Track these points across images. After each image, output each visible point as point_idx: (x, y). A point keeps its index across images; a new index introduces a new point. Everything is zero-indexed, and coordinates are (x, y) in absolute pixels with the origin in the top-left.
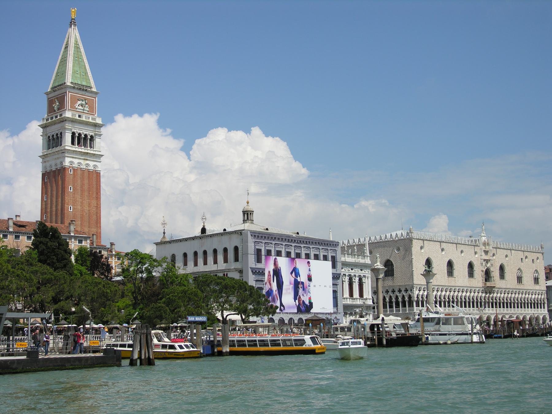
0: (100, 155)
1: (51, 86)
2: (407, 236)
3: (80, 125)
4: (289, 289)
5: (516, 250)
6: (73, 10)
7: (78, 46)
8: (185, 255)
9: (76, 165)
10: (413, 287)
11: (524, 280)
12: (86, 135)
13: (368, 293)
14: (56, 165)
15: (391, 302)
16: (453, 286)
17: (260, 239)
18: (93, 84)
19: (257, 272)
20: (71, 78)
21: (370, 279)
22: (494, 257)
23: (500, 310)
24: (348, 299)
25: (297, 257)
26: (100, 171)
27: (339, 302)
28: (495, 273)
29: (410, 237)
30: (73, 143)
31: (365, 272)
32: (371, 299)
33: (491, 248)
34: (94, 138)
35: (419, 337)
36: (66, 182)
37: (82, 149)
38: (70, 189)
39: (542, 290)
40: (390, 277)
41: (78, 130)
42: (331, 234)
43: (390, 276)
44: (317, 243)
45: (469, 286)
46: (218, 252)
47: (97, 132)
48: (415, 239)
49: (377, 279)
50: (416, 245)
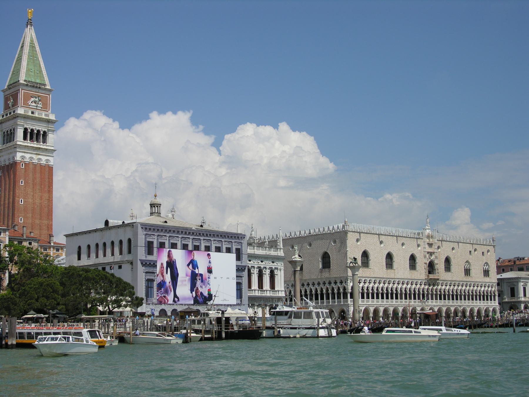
0: (52, 150)
1: (7, 84)
2: (342, 229)
3: (33, 121)
4: (186, 281)
5: (464, 243)
6: (30, 11)
7: (33, 45)
8: (89, 247)
9: (27, 160)
10: (347, 279)
11: (472, 272)
12: (39, 131)
13: (280, 285)
14: (9, 159)
17: (152, 232)
18: (47, 81)
19: (148, 264)
20: (25, 76)
21: (282, 272)
22: (439, 250)
24: (256, 291)
26: (52, 165)
27: (243, 294)
28: (440, 266)
29: (346, 229)
30: (25, 138)
31: (277, 264)
32: (283, 291)
34: (47, 134)
35: (260, 331)
36: (17, 176)
37: (34, 144)
38: (21, 183)
40: (327, 269)
41: (30, 126)
42: (239, 226)
44: (219, 236)
45: (410, 278)
47: (50, 127)
48: (350, 232)
50: (351, 238)
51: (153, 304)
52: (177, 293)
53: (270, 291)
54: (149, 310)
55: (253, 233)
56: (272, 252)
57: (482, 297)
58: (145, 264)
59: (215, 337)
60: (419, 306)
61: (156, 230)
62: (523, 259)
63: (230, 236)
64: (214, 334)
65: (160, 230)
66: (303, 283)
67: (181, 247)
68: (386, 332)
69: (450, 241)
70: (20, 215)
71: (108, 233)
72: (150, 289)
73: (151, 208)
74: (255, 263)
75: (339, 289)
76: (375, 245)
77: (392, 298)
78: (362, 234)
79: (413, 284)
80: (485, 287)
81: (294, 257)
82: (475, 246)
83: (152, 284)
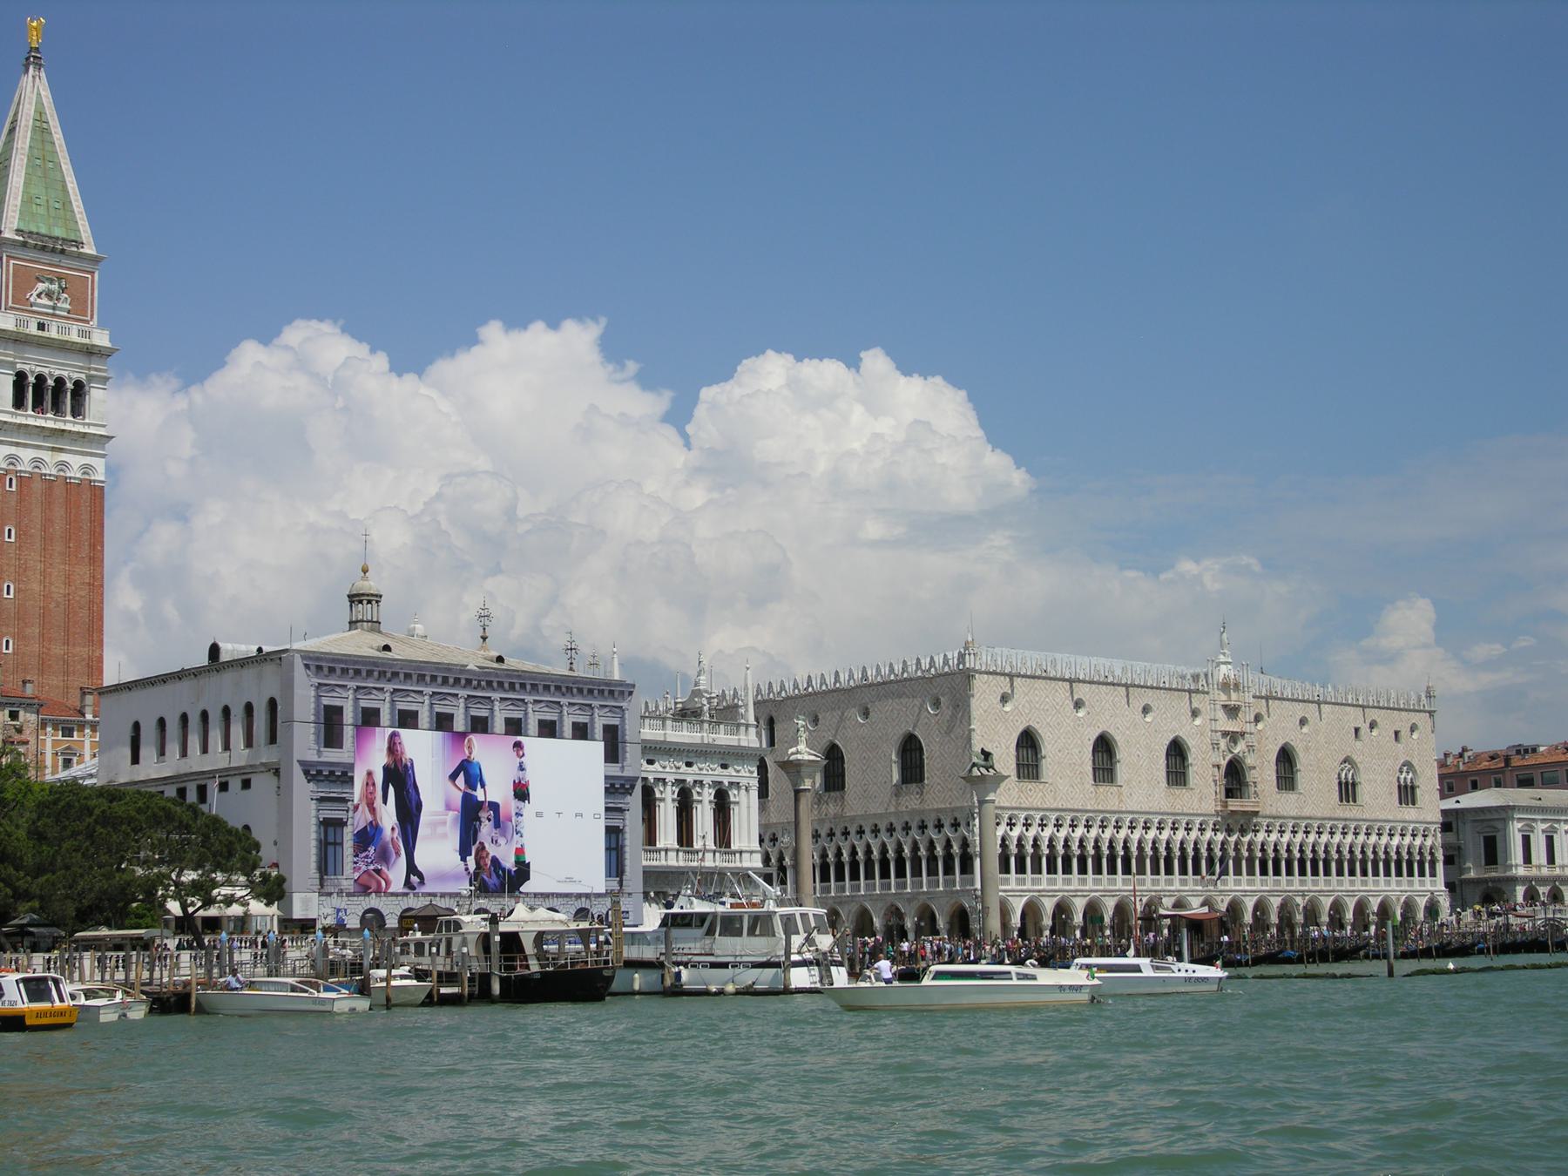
0: (101, 436)
3: (41, 350)
6: (35, 24)
7: (45, 126)
8: (162, 723)
9: (25, 467)
10: (973, 815)
11: (1364, 792)
12: (60, 381)
15: (949, 858)
16: (1114, 812)
18: (85, 232)
22: (1260, 726)
24: (669, 853)
25: (474, 730)
28: (1263, 773)
29: (968, 665)
30: (19, 402)
31: (738, 771)
33: (1248, 698)
34: (87, 388)
35: (606, 973)
37: (46, 419)
40: (914, 785)
44: (552, 689)
45: (1169, 811)
47: (96, 370)
48: (981, 673)
49: (797, 792)
50: (984, 694)
51: (340, 893)
52: (420, 861)
53: (714, 852)
54: (330, 911)
55: (702, 678)
56: (722, 736)
57: (1393, 865)
58: (314, 773)
59: (471, 995)
62: (1534, 750)
63: (586, 688)
64: (466, 984)
65: (364, 674)
66: (846, 828)
67: (430, 723)
68: (933, 979)
69: (1293, 700)
72: (331, 849)
73: (351, 606)
74: (668, 770)
75: (948, 845)
77: (1112, 870)
78: (1017, 681)
79: (1177, 829)
80: (1402, 835)
81: (794, 750)
82: (1373, 714)
83: (338, 836)
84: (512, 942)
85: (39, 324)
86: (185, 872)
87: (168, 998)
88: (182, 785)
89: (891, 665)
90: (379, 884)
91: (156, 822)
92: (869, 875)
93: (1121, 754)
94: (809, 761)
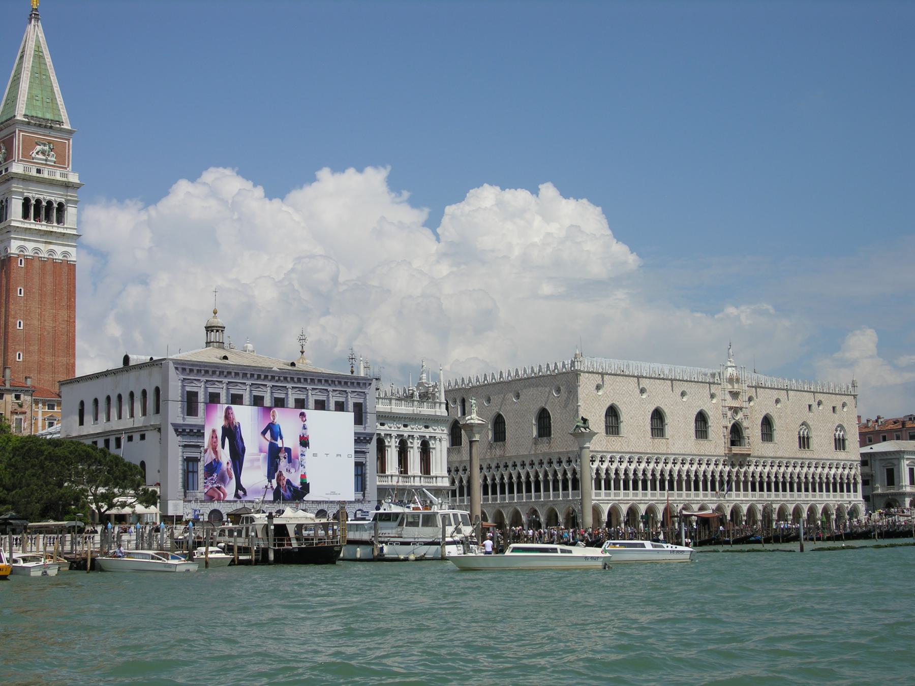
0: (74, 235)
5: (798, 391)
7: (41, 54)
9: (29, 253)
11: (814, 442)
12: (50, 203)
16: (664, 454)
18: (64, 116)
20: (25, 108)
22: (752, 404)
23: (806, 495)
24: (393, 478)
25: (276, 406)
27: (368, 483)
28: (753, 431)
29: (576, 368)
30: (26, 215)
31: (435, 430)
33: (745, 387)
34: (65, 207)
35: (336, 549)
36: (11, 280)
37: (42, 225)
38: (20, 292)
39: (853, 461)
40: (545, 438)
43: (547, 436)
44: (323, 381)
46: (135, 398)
47: (71, 196)
48: (584, 372)
50: (586, 385)
51: (196, 501)
53: (420, 477)
54: (190, 511)
56: (425, 409)
58: (180, 431)
60: (712, 502)
61: (203, 372)
64: (254, 554)
65: (210, 373)
66: (506, 463)
67: (250, 401)
68: (512, 551)
70: (17, 347)
71: (125, 376)
72: (190, 475)
73: (207, 333)
74: (393, 429)
75: (565, 473)
76: (630, 395)
78: (606, 377)
79: (701, 464)
80: (837, 468)
81: (469, 417)
82: (820, 397)
83: (195, 467)
84: (281, 530)
85: (37, 170)
86: (99, 489)
87: (80, 562)
88: (107, 438)
89: (532, 368)
90: (219, 495)
91: (81, 460)
92: (520, 491)
93: (668, 420)
94: (478, 424)
